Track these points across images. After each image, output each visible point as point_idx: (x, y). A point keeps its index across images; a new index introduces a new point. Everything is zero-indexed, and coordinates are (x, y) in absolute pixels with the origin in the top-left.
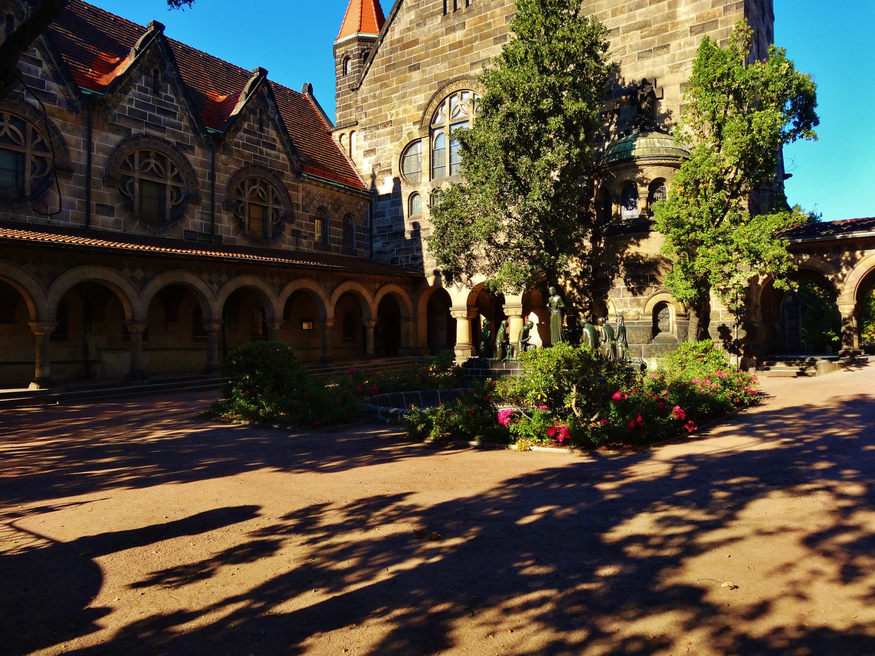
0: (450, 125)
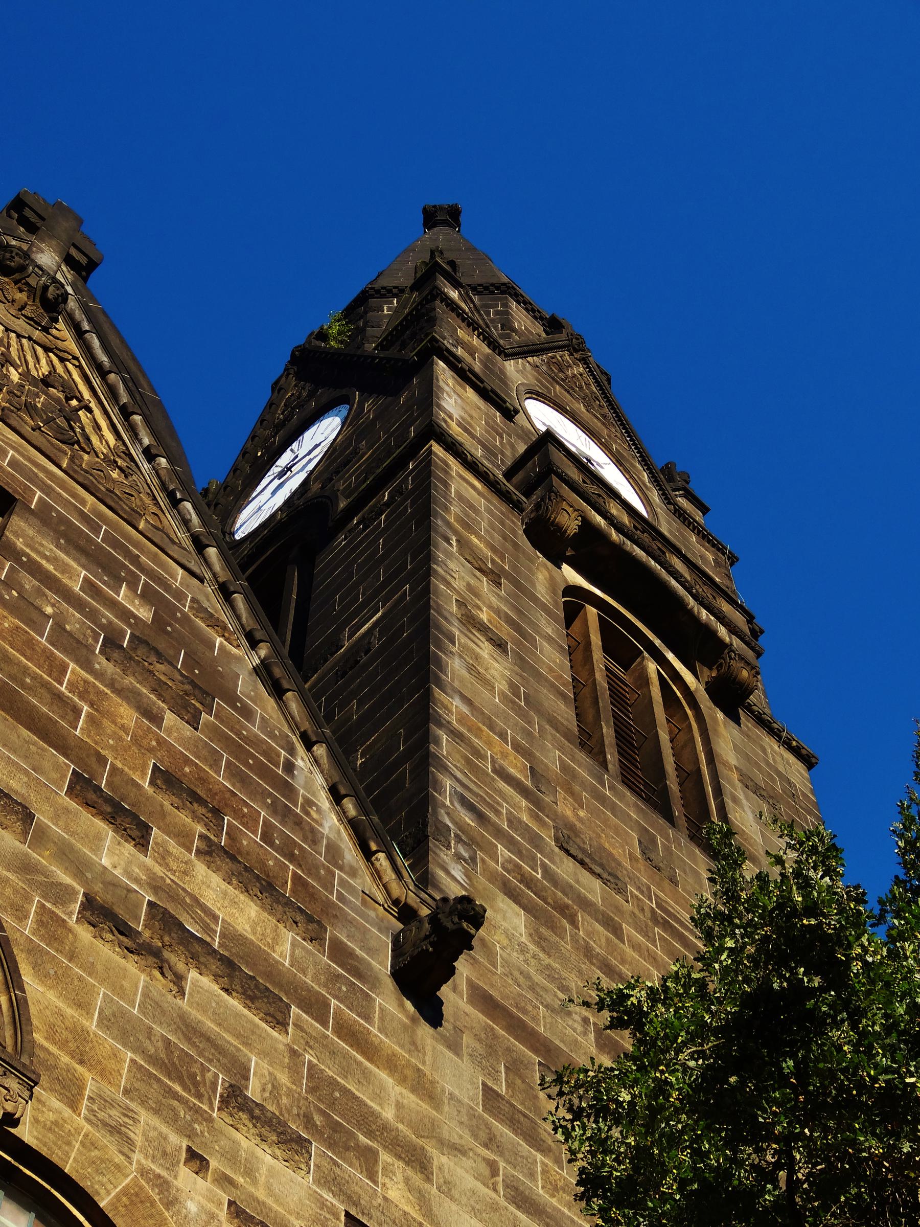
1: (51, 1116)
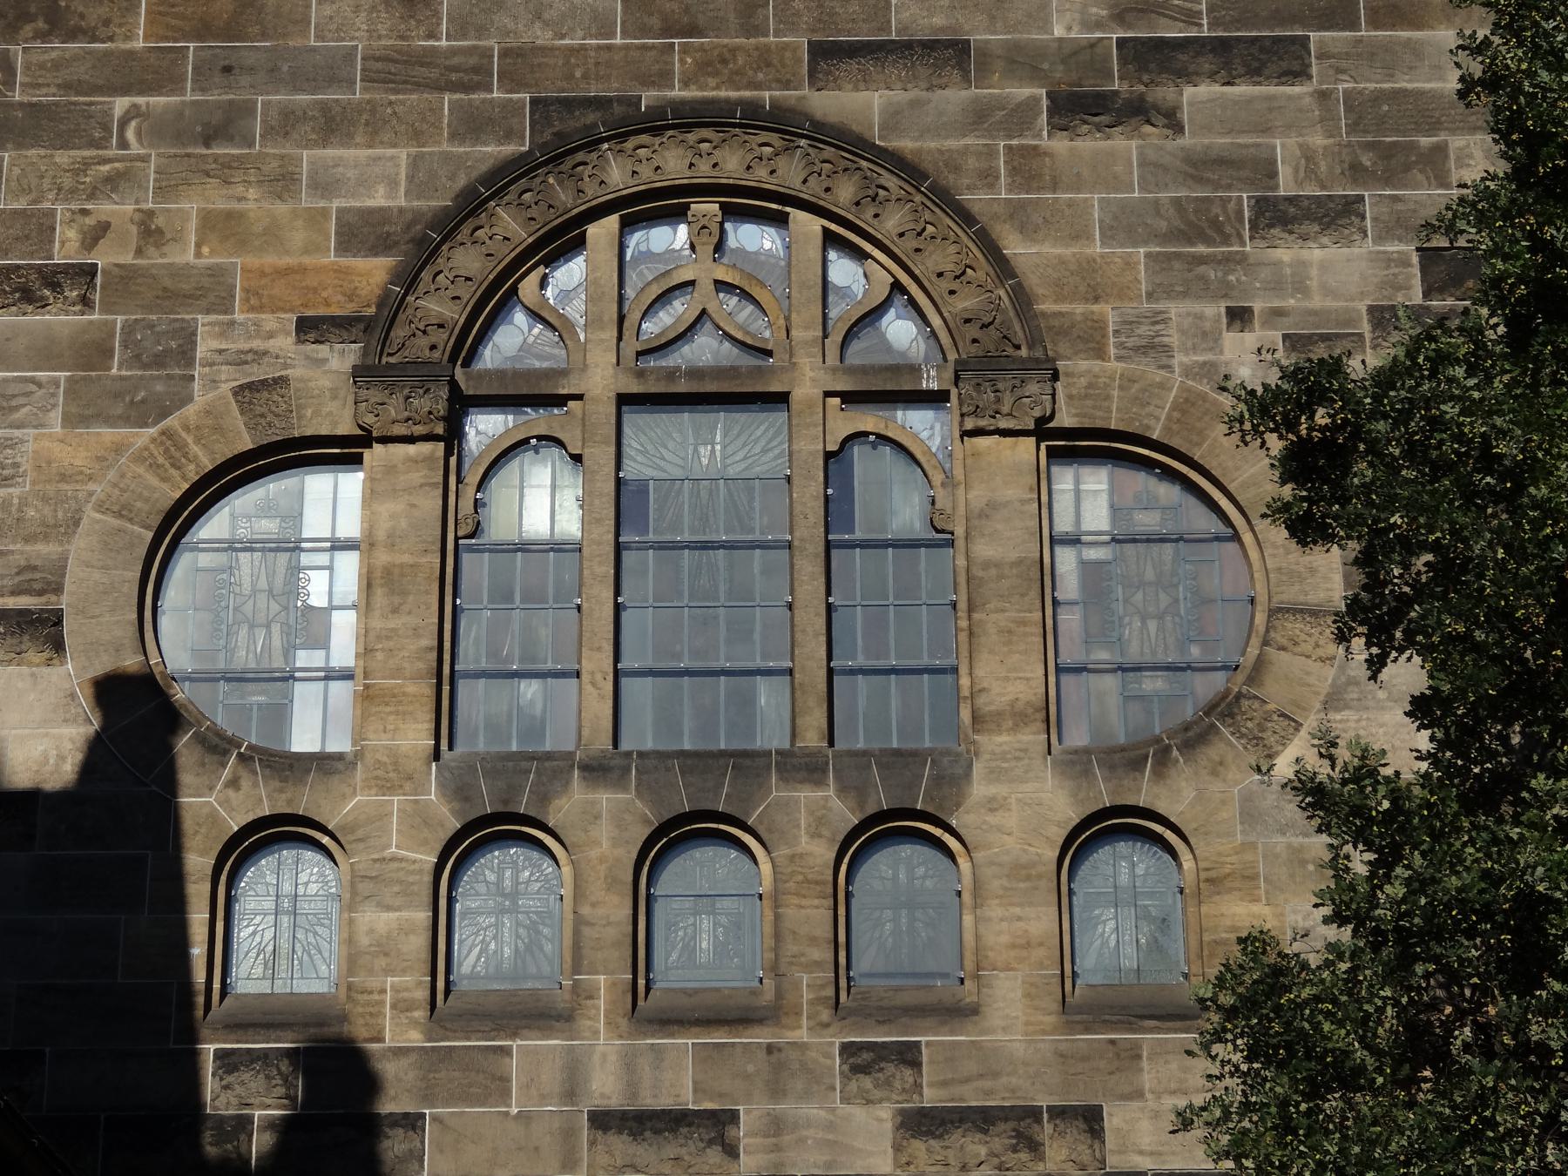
1: (1083, 381)
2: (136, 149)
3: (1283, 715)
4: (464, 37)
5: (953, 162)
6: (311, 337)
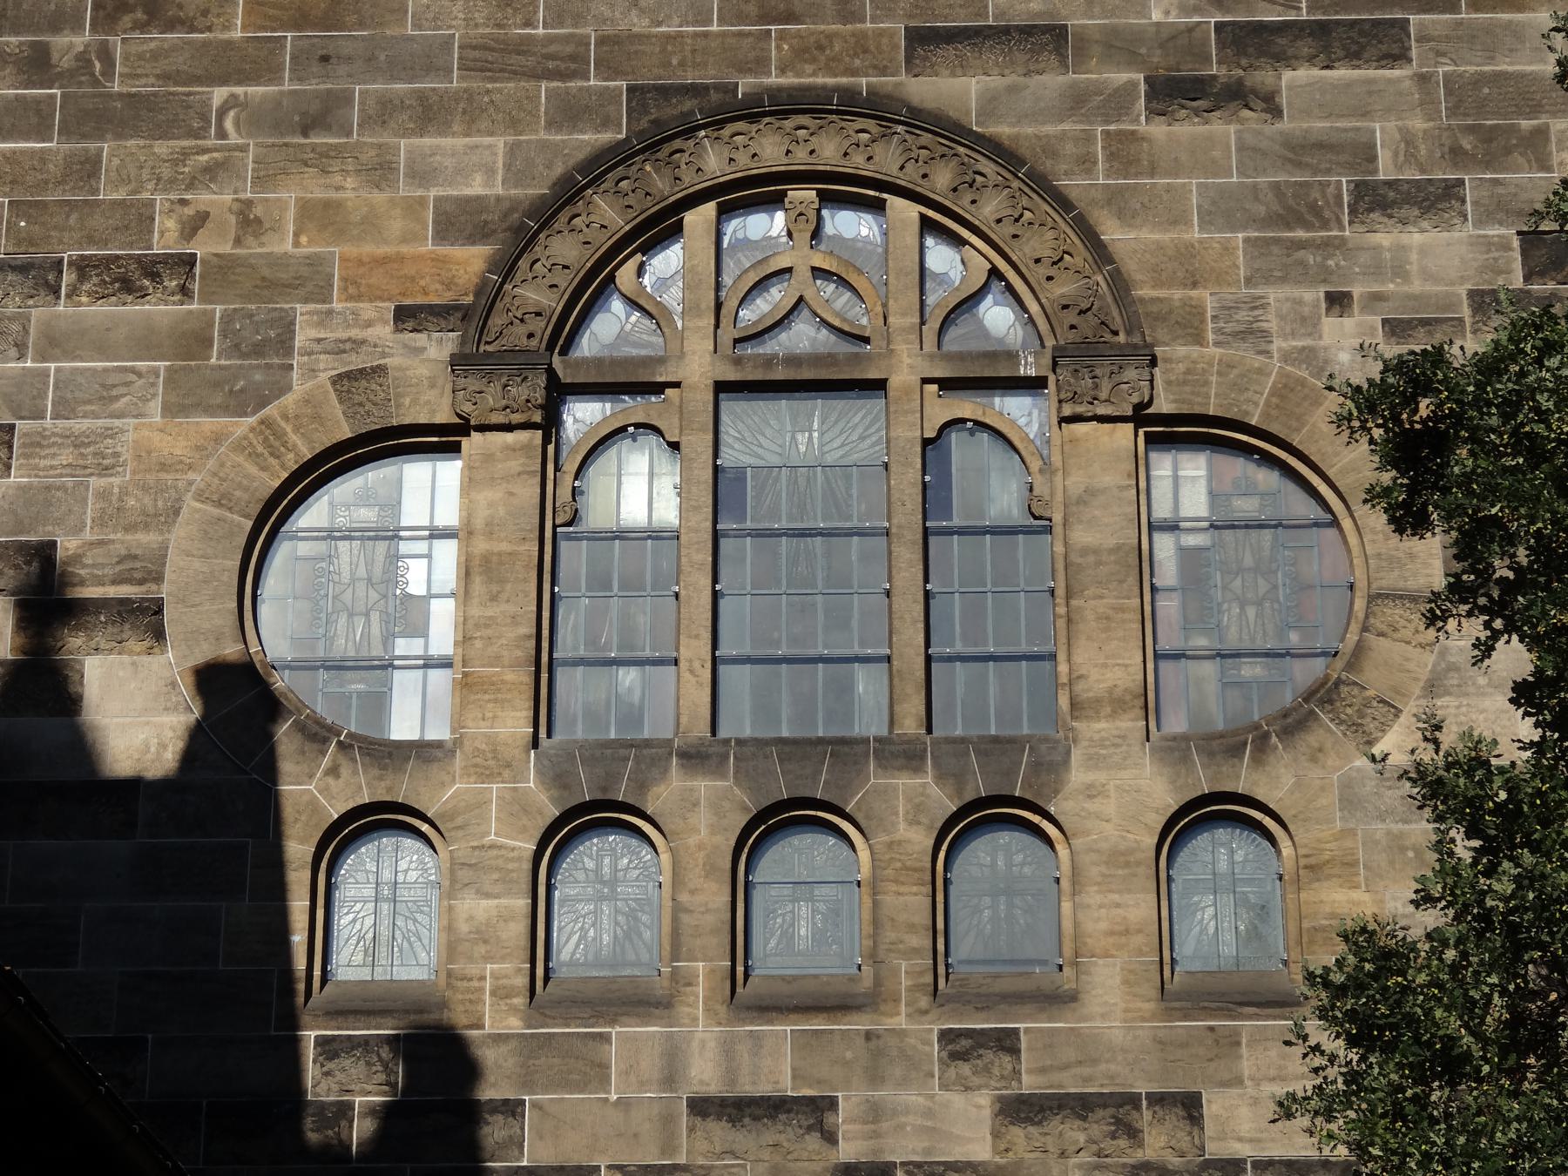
0: (721, 387)
1: (1181, 367)
2: (234, 139)
3: (1382, 701)
4: (561, 25)
5: (1050, 148)
6: (410, 325)
